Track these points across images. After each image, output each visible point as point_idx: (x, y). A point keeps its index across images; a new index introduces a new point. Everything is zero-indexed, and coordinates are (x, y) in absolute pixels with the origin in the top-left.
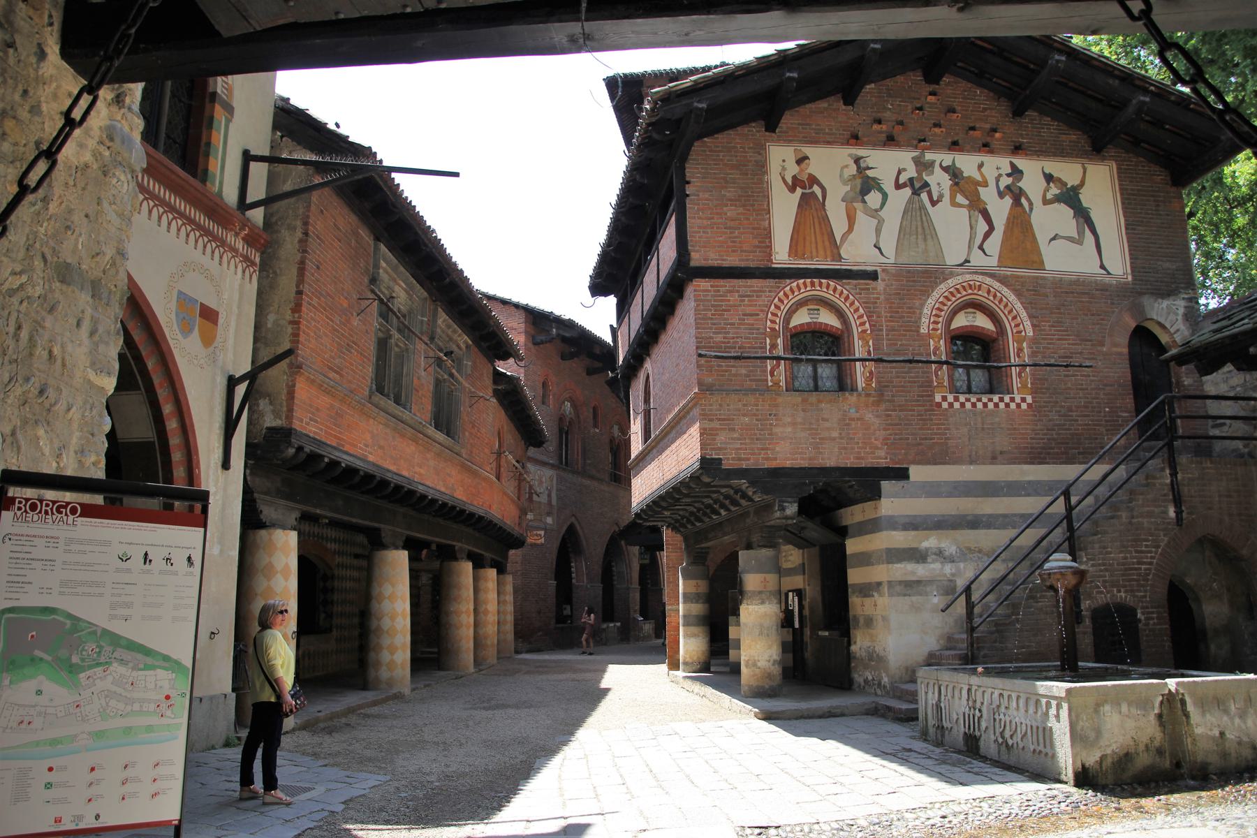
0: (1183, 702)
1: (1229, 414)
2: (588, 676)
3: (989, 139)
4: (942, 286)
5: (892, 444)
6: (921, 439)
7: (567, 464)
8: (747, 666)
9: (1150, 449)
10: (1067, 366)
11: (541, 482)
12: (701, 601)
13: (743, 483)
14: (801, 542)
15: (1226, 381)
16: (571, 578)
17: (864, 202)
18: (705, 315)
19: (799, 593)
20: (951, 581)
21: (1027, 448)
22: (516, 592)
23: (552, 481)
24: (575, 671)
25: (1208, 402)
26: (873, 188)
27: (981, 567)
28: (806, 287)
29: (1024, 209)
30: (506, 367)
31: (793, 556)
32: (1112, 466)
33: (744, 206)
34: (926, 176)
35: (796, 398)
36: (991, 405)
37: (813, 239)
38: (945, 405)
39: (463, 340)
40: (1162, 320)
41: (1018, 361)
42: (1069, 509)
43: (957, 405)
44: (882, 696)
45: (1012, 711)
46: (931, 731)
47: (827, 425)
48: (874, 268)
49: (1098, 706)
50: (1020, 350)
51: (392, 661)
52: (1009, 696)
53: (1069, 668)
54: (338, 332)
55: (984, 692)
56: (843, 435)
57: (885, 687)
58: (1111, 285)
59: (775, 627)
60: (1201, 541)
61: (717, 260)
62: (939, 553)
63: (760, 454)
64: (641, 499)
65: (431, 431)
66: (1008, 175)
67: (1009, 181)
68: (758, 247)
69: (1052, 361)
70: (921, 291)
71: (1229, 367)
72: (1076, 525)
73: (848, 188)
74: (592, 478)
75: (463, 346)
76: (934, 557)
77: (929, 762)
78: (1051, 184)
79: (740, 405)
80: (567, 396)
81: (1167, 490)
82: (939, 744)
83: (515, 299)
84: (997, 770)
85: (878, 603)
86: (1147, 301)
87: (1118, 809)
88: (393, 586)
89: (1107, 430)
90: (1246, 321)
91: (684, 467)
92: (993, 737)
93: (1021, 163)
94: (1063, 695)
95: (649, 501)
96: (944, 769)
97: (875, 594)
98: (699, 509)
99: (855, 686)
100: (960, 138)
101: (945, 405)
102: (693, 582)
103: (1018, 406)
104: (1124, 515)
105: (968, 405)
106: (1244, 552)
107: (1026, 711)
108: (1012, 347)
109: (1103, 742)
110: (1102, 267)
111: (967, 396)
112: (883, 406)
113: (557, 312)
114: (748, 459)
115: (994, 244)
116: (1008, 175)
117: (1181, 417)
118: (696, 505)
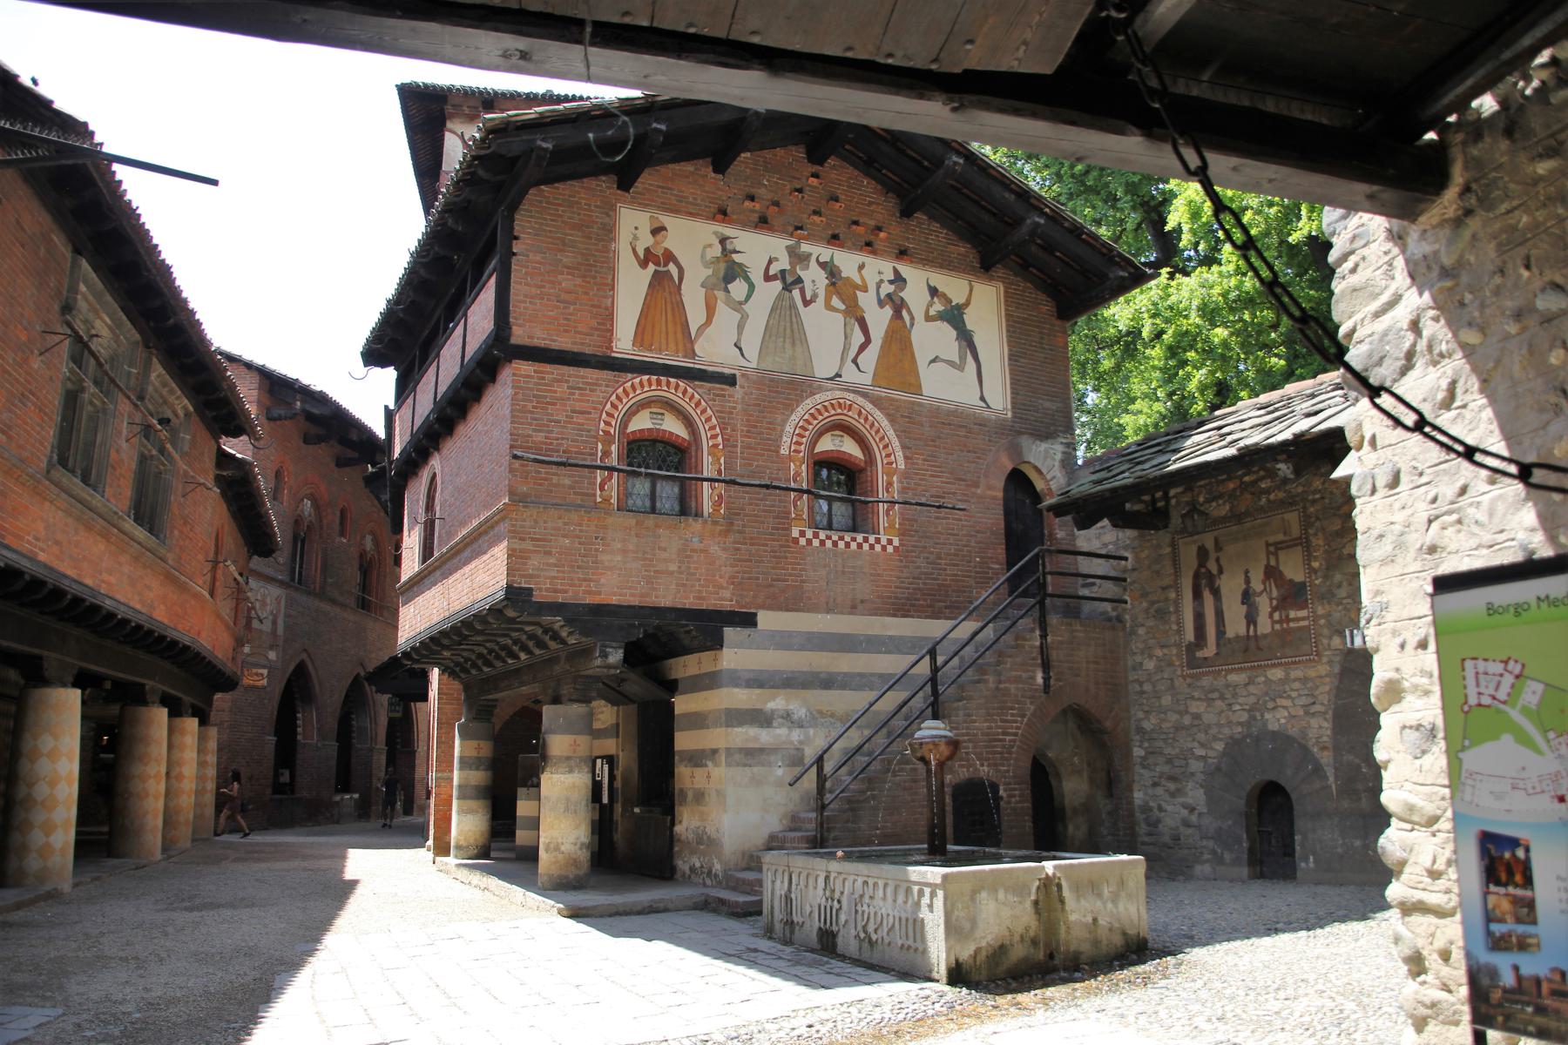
0: (1059, 886)
1: (1099, 573)
2: (324, 863)
3: (872, 238)
4: (808, 401)
5: (740, 584)
6: (773, 580)
7: (300, 582)
8: (547, 850)
9: (1019, 607)
10: (939, 507)
13: (557, 621)
14: (616, 695)
15: (1098, 537)
17: (728, 291)
18: (524, 406)
19: (610, 760)
20: (798, 749)
21: (890, 598)
22: (220, 750)
23: (279, 603)
24: (305, 857)
25: (1080, 558)
26: (739, 276)
27: (834, 735)
28: (650, 385)
29: (904, 322)
30: (235, 447)
31: (606, 714)
32: (980, 624)
33: (584, 276)
34: (802, 269)
35: (631, 520)
36: (854, 545)
37: (664, 329)
38: (803, 541)
39: (181, 404)
40: (1039, 465)
41: (886, 497)
42: (935, 670)
43: (816, 543)
44: (712, 886)
45: (878, 902)
46: (778, 926)
47: (666, 555)
48: (732, 372)
49: (974, 893)
50: (890, 484)
51: (48, 845)
52: (875, 884)
53: (937, 853)
54: (10, 375)
55: (844, 880)
56: (683, 568)
57: (716, 876)
58: (989, 420)
59: (584, 803)
60: (1064, 712)
61: (544, 339)
62: (787, 716)
63: (580, 586)
64: (413, 634)
65: (129, 525)
66: (891, 282)
67: (891, 288)
68: (597, 329)
69: (923, 500)
70: (783, 404)
71: (1105, 522)
72: (941, 689)
73: (710, 272)
74: (333, 602)
75: (181, 413)
76: (780, 720)
77: (782, 964)
78: (936, 299)
79: (560, 523)
81: (1036, 653)
82: (787, 942)
83: (248, 356)
84: (860, 970)
85: (712, 775)
86: (1025, 441)
87: (995, 1007)
88: (56, 738)
89: (977, 583)
90: (1127, 474)
91: (480, 596)
92: (853, 932)
93: (906, 270)
94: (939, 881)
95: (424, 637)
96: (799, 970)
97: (709, 763)
98: (491, 651)
99: (678, 875)
100: (841, 231)
101: (803, 541)
102: (474, 743)
103: (884, 548)
104: (991, 678)
105: (829, 544)
106: (1108, 724)
107: (895, 901)
108: (881, 480)
109: (978, 933)
110: (982, 399)
111: (828, 532)
112: (731, 538)
113: (305, 381)
114: (566, 592)
115: (870, 358)
116: (891, 282)
117: (1051, 573)
118: (488, 645)
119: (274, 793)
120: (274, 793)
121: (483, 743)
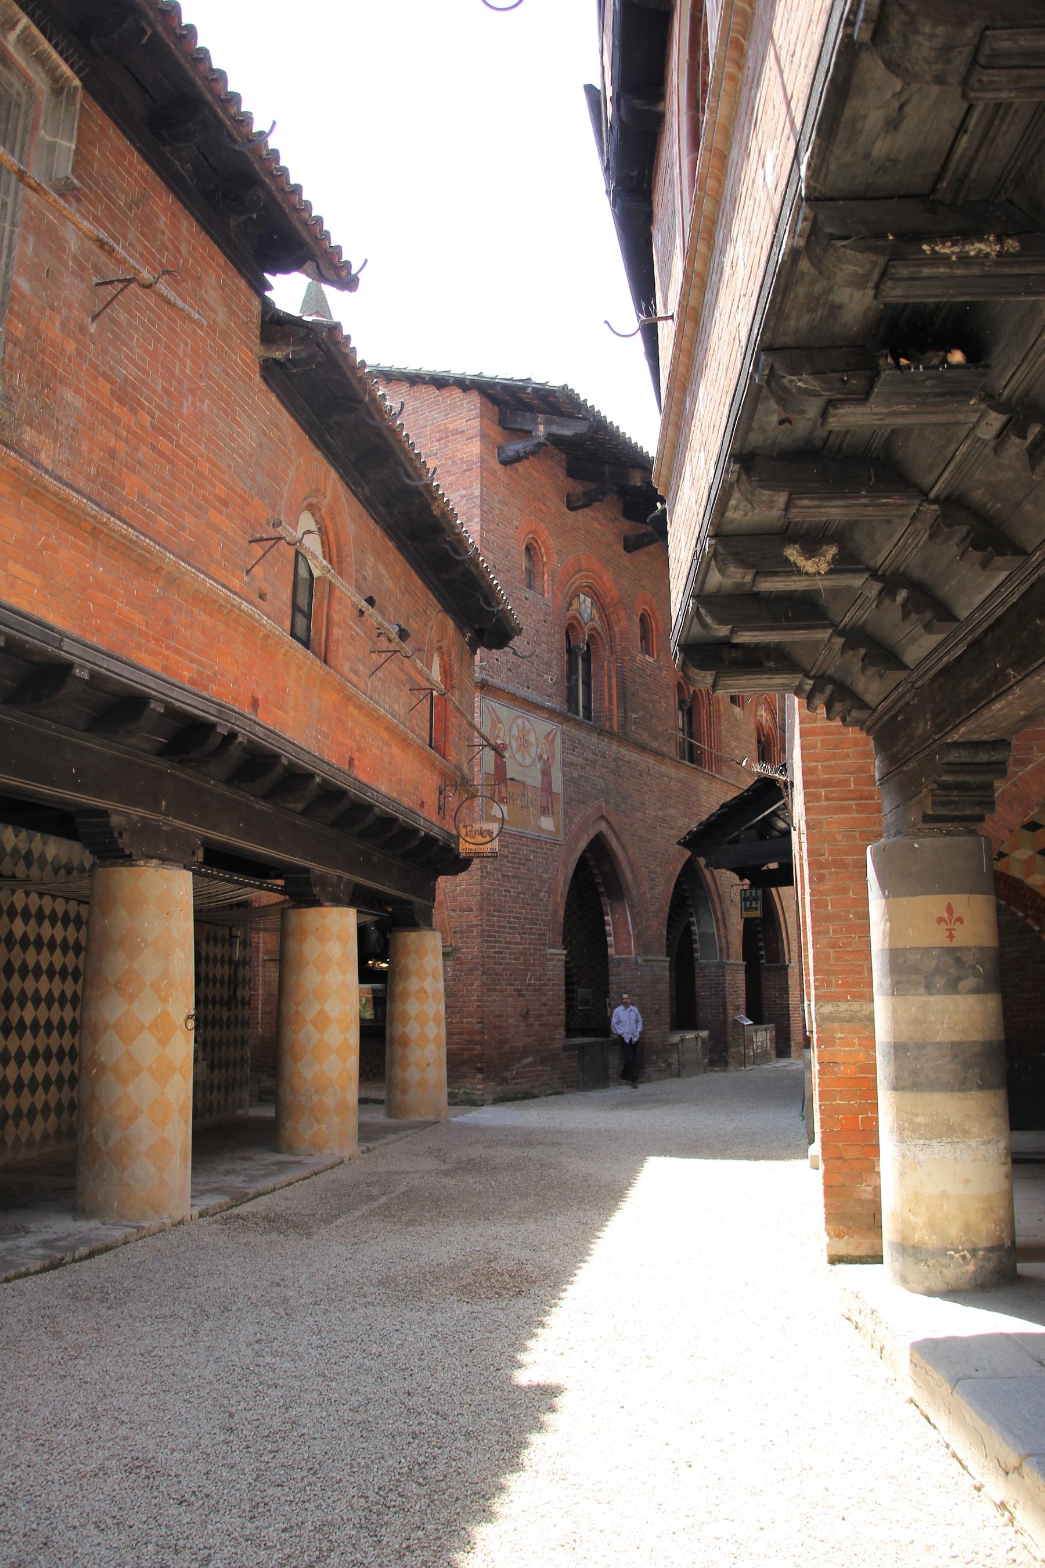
7: (588, 715)
11: (524, 743)
12: (970, 982)
16: (605, 945)
23: (552, 743)
74: (641, 747)
80: (584, 582)
102: (934, 904)
119: (568, 1036)
120: (570, 1032)
121: (960, 902)
